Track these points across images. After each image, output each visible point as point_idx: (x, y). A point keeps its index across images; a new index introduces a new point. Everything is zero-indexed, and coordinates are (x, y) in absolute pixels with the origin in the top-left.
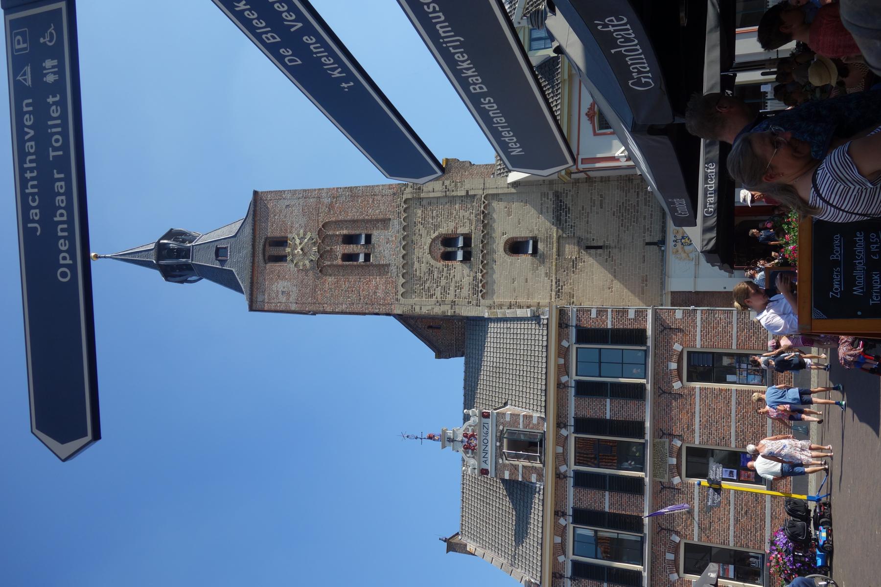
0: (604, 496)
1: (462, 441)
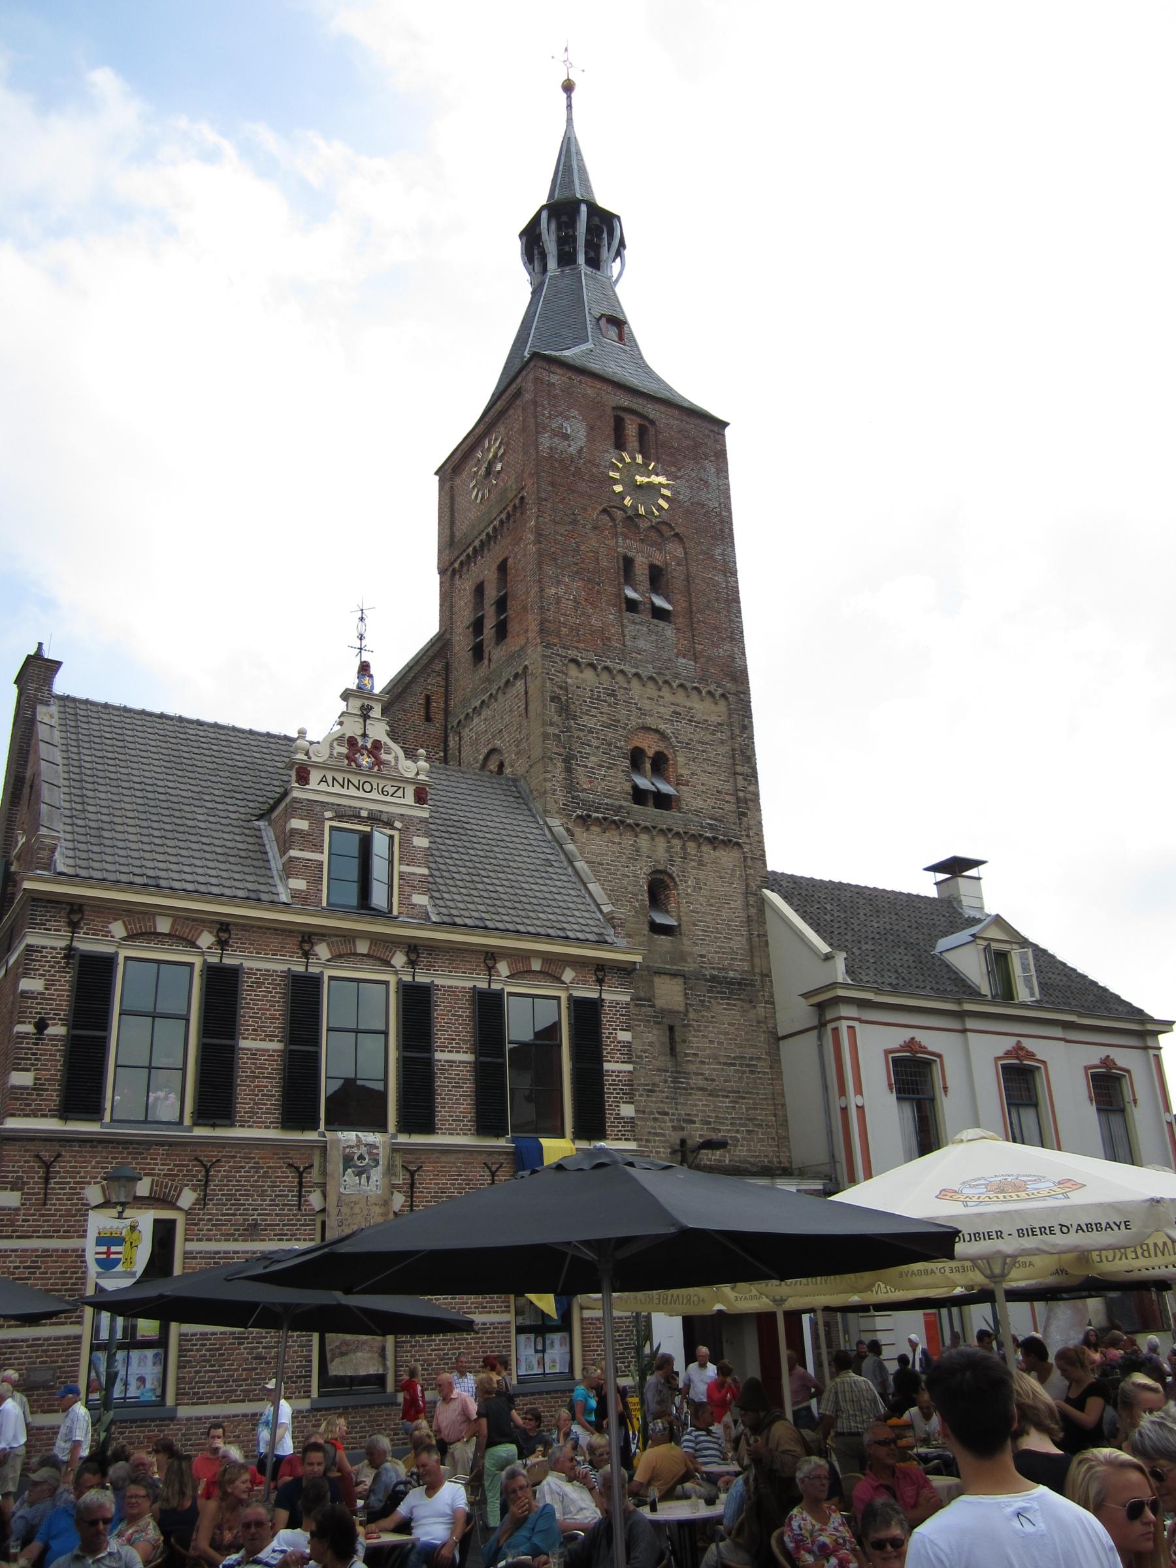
0: (271, 1038)
1: (364, 735)
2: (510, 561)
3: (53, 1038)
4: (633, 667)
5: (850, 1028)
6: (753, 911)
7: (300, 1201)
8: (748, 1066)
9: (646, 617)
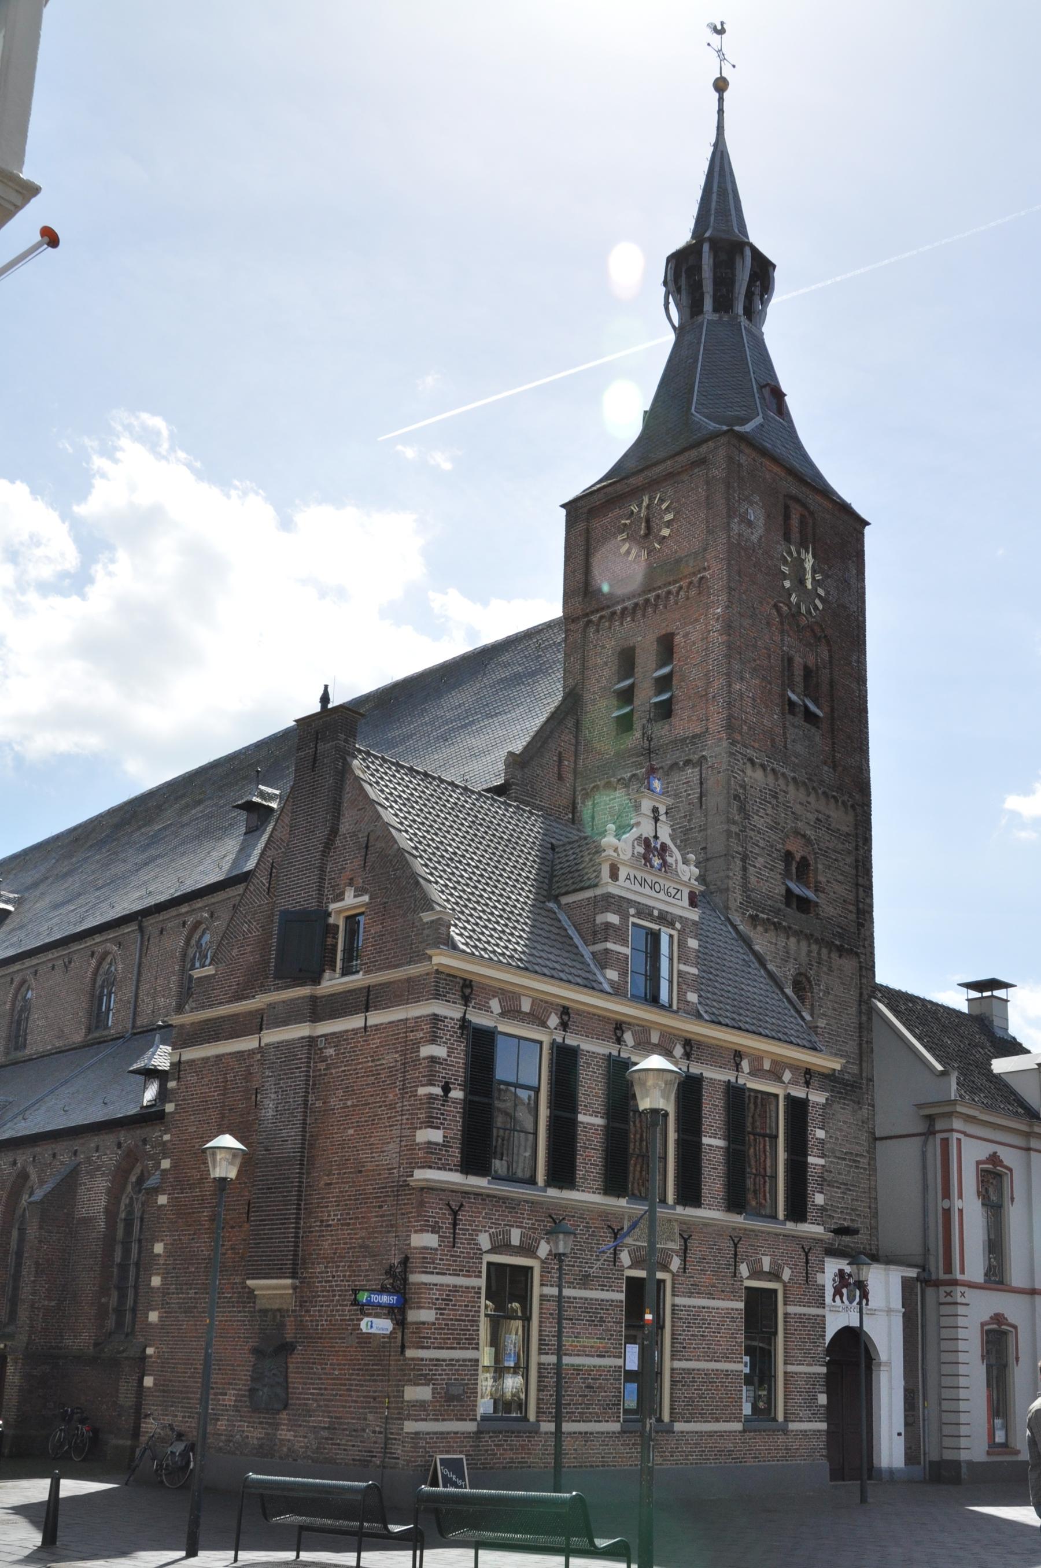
1: (656, 837)
2: (678, 639)
3: (455, 1101)
4: (792, 771)
5: (959, 1140)
6: (864, 1018)
7: (615, 1258)
8: (855, 1161)
9: (799, 720)
